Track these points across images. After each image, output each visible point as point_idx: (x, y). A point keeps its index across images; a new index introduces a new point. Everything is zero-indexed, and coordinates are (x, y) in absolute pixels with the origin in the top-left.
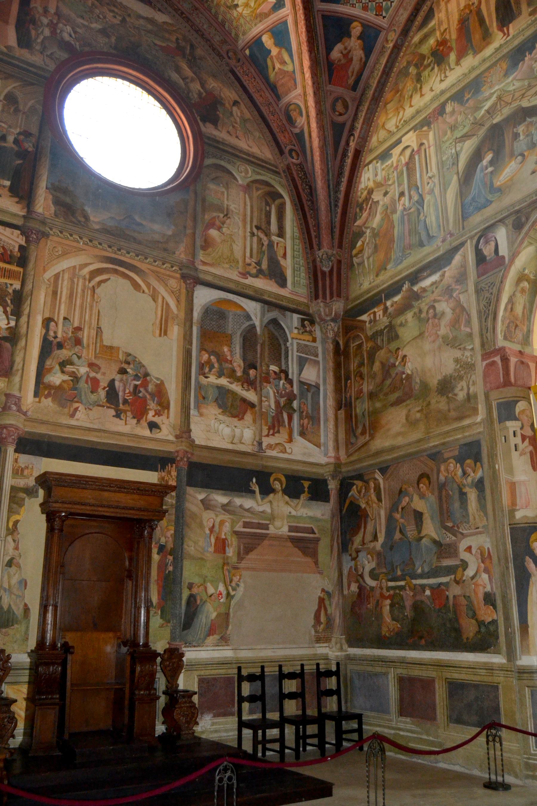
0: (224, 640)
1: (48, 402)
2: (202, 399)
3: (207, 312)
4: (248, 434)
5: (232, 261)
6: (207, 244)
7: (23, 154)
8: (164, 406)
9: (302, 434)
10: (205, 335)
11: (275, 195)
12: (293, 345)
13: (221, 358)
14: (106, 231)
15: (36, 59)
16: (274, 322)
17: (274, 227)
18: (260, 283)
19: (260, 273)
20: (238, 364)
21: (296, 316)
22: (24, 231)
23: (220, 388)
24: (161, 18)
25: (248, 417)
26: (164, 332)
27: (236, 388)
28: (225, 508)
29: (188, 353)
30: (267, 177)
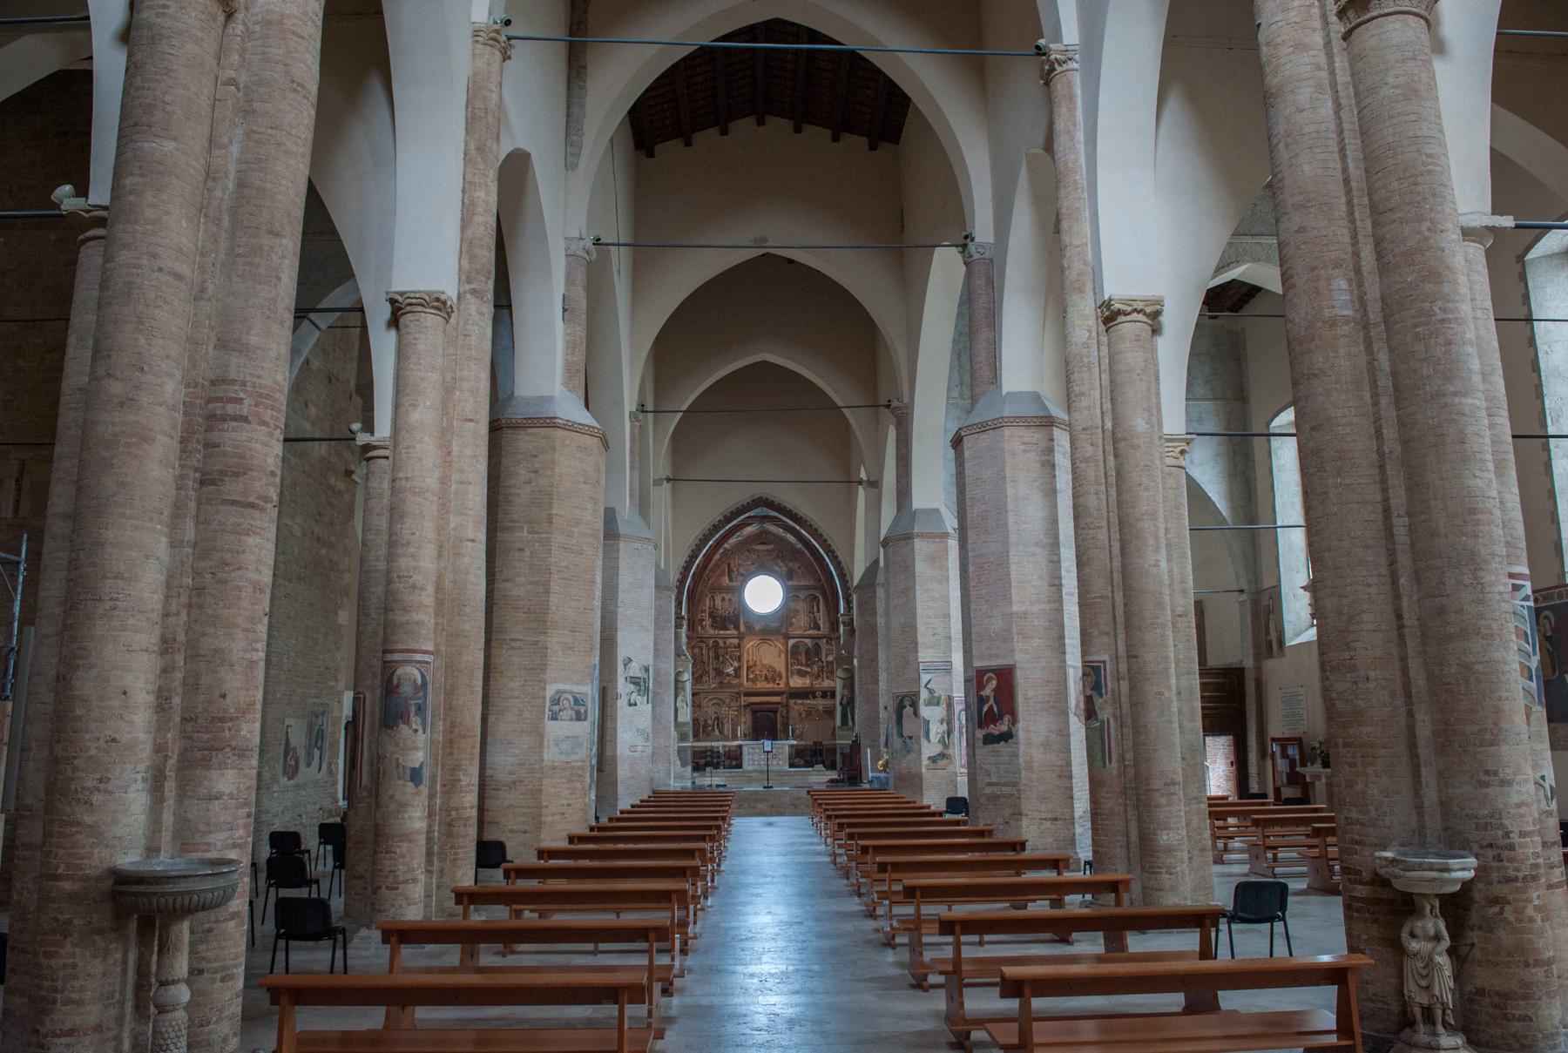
0: (802, 740)
1: (750, 683)
2: (792, 674)
3: (793, 646)
4: (808, 682)
5: (801, 628)
6: (792, 624)
7: (735, 616)
8: (781, 678)
9: (827, 678)
10: (792, 655)
11: (816, 598)
12: (824, 651)
13: (798, 660)
14: (760, 631)
15: (734, 584)
16: (817, 644)
17: (815, 610)
18: (811, 632)
19: (811, 628)
20: (804, 660)
21: (825, 640)
22: (739, 638)
23: (799, 670)
24: (771, 547)
25: (808, 677)
26: (780, 656)
27: (804, 668)
28: (802, 704)
29: (787, 661)
30: (813, 592)
